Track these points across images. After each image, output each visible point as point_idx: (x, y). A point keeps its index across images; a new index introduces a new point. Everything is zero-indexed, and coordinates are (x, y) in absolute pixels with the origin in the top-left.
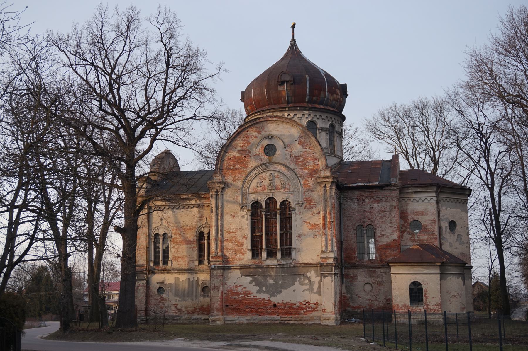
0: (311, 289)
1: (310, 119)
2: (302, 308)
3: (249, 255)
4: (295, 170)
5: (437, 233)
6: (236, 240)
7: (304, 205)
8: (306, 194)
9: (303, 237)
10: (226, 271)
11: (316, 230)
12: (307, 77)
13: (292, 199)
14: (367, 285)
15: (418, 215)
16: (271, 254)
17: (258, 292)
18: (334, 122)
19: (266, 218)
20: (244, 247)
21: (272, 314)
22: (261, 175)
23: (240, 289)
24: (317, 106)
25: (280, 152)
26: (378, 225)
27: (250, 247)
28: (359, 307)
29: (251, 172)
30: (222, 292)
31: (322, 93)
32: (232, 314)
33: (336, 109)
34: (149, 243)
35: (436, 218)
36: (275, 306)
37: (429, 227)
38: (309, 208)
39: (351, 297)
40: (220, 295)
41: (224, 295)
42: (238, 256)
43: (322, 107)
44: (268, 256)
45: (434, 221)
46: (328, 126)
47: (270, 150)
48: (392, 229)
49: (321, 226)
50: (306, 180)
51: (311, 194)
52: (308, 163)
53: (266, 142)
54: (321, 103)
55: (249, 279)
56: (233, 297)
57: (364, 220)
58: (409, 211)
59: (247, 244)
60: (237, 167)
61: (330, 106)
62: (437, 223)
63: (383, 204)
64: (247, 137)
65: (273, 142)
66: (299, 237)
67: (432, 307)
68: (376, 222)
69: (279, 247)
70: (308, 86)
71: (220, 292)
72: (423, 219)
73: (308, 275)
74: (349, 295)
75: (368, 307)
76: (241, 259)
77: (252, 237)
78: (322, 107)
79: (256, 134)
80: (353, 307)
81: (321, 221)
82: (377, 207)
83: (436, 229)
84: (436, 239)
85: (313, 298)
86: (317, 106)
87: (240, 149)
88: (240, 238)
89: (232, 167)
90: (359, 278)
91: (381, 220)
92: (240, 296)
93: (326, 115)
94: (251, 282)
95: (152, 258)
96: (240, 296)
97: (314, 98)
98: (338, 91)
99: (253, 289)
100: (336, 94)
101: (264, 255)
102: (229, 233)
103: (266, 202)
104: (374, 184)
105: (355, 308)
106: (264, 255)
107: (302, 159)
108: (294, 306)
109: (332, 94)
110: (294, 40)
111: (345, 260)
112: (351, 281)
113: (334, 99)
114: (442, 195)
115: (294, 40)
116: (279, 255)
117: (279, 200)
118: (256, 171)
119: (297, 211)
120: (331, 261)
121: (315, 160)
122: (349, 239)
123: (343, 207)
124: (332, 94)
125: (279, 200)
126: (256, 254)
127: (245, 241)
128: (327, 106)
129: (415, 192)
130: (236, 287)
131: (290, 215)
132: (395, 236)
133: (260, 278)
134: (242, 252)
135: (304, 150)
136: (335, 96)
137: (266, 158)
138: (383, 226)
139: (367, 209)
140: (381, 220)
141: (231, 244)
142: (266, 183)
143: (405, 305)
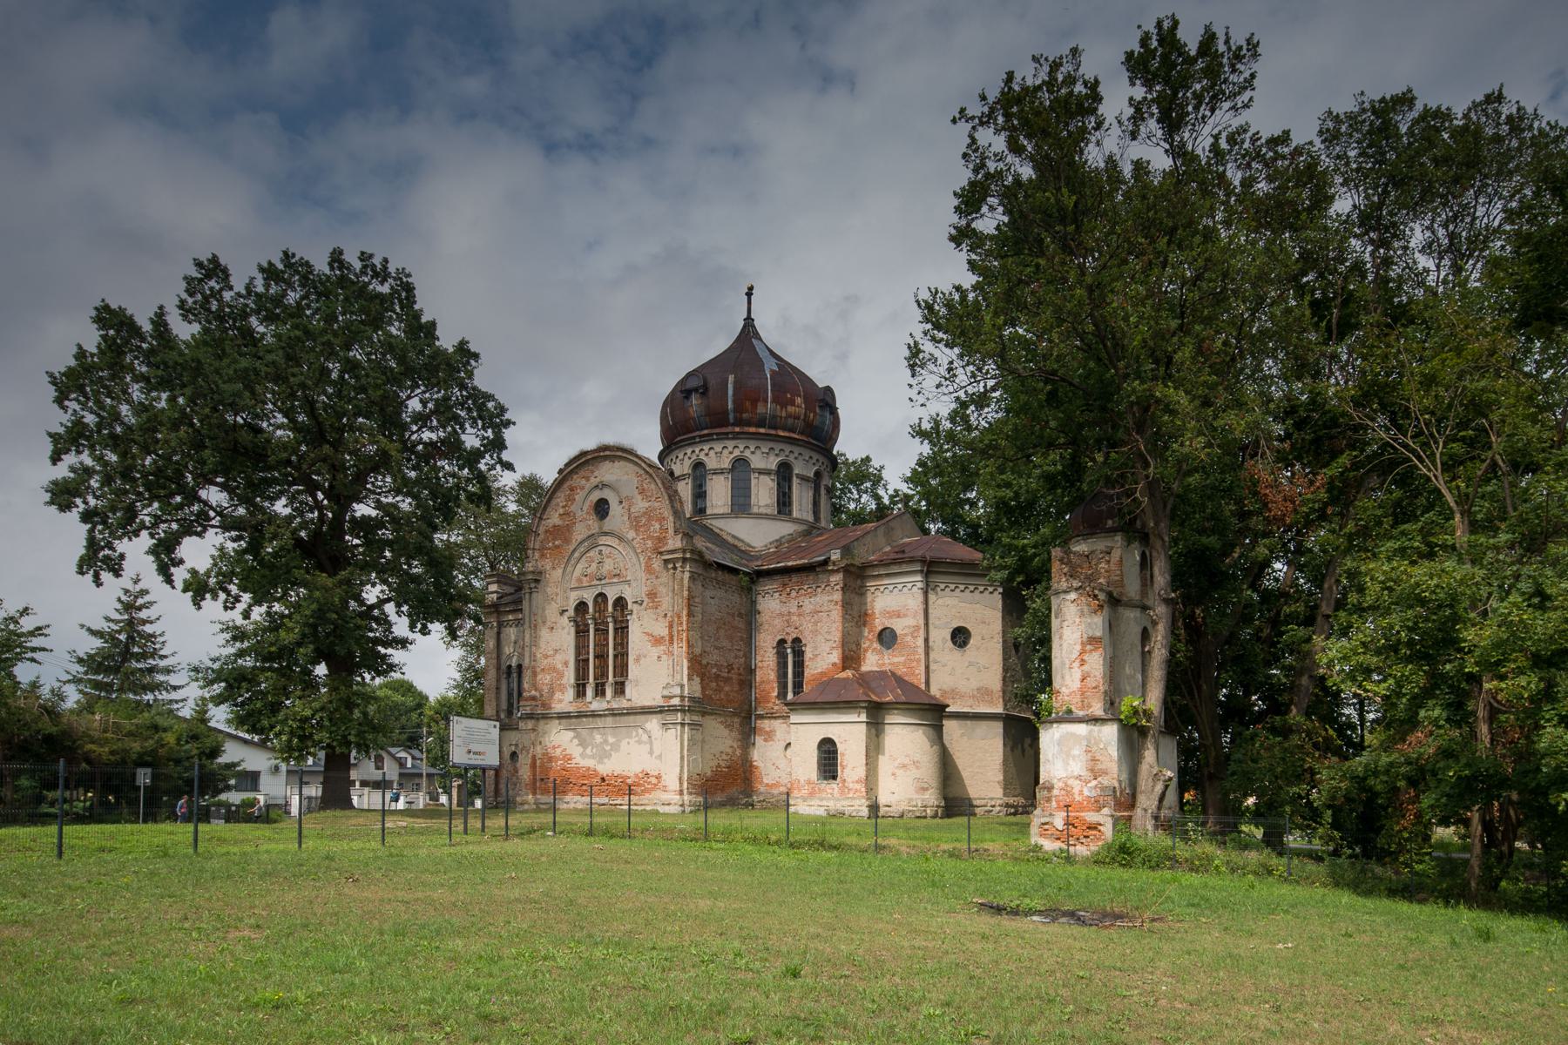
0: (651, 752)
1: (737, 453)
2: (638, 785)
3: (570, 694)
5: (921, 650)
10: (542, 722)
12: (731, 378)
16: (600, 691)
17: (583, 755)
18: (791, 458)
19: (596, 630)
20: (564, 681)
24: (752, 430)
25: (615, 509)
30: (534, 757)
33: (802, 433)
34: (498, 681)
35: (922, 622)
36: (603, 779)
43: (762, 430)
45: (917, 628)
46: (774, 467)
47: (601, 508)
54: (761, 424)
55: (571, 734)
59: (570, 677)
61: (784, 429)
62: (922, 633)
66: (637, 660)
68: (806, 633)
70: (730, 392)
72: (899, 626)
73: (648, 726)
77: (577, 661)
78: (762, 430)
79: (583, 482)
81: (665, 632)
82: (809, 604)
83: (920, 642)
84: (918, 661)
85: (652, 766)
86: (752, 430)
88: (559, 666)
93: (771, 445)
95: (504, 706)
98: (799, 400)
100: (793, 404)
102: (546, 657)
109: (784, 405)
110: (749, 320)
113: (789, 416)
115: (749, 320)
116: (609, 692)
120: (676, 701)
121: (662, 519)
126: (580, 691)
128: (775, 428)
129: (888, 575)
133: (584, 733)
134: (562, 689)
136: (791, 409)
139: (794, 610)
143: (809, 782)
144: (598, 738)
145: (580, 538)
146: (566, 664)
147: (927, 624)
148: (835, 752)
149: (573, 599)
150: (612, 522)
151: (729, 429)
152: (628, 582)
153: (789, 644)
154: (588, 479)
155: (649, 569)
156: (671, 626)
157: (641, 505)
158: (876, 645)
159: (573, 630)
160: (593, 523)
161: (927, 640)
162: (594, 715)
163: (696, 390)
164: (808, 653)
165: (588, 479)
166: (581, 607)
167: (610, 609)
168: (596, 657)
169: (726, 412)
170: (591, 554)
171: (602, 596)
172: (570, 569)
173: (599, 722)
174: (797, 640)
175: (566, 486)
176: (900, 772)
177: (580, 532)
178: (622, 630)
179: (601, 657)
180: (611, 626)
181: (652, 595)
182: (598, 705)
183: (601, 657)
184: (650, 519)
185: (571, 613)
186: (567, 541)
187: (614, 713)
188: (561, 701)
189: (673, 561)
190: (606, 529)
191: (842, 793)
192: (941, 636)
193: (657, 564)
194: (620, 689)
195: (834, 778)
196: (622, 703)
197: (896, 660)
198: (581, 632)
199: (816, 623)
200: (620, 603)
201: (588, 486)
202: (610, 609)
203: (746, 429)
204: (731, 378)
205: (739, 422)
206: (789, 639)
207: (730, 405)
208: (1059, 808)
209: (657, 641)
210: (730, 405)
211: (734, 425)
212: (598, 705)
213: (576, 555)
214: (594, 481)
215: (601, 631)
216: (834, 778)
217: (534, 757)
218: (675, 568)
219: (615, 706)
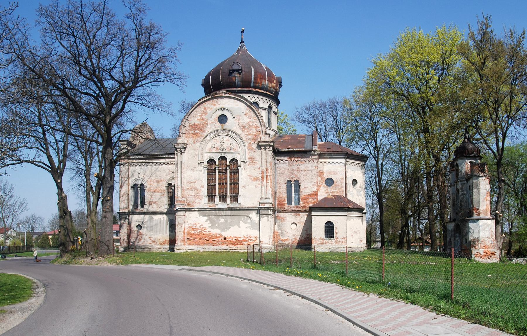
2: (245, 241)
4: (242, 136)
6: (195, 189)
7: (248, 163)
8: (250, 154)
9: (247, 187)
11: (258, 182)
13: (238, 157)
14: (294, 225)
15: (331, 174)
19: (219, 172)
20: (202, 194)
21: (223, 244)
22: (215, 138)
23: (198, 226)
24: (259, 91)
26: (302, 180)
27: (206, 194)
28: (287, 240)
29: (207, 136)
30: (184, 229)
31: (263, 81)
32: (192, 244)
36: (225, 238)
37: (339, 183)
38: (252, 165)
39: (282, 233)
40: (183, 230)
41: (186, 230)
42: (197, 200)
43: (263, 91)
44: (220, 200)
47: (222, 119)
48: (313, 183)
49: (261, 178)
50: (250, 143)
51: (254, 154)
52: (252, 131)
53: (220, 113)
54: (262, 89)
55: (206, 218)
56: (193, 232)
57: (292, 176)
58: (325, 171)
60: (196, 131)
63: (307, 165)
64: (205, 108)
65: (225, 113)
67: (340, 240)
68: (301, 178)
69: (229, 194)
71: (183, 228)
73: (251, 216)
74: (280, 231)
75: (293, 240)
76: (199, 203)
78: (263, 91)
79: (212, 106)
80: (282, 240)
81: (260, 175)
84: (343, 192)
86: (259, 91)
87: (199, 117)
88: (198, 187)
89: (193, 132)
90: (287, 219)
91: (305, 177)
92: (199, 231)
94: (206, 221)
96: (199, 231)
97: (257, 84)
98: (275, 81)
99: (207, 225)
101: (217, 199)
103: (219, 159)
104: (300, 149)
105: (284, 241)
106: (217, 199)
107: (247, 127)
108: (239, 239)
109: (271, 82)
111: (278, 206)
112: (282, 221)
114: (348, 160)
116: (228, 200)
117: (229, 158)
118: (211, 136)
119: (242, 167)
120: (267, 205)
122: (281, 190)
123: (277, 166)
124: (271, 82)
125: (229, 158)
127: (203, 189)
130: (196, 224)
131: (238, 169)
132: (315, 189)
133: (214, 218)
134: (200, 198)
135: (249, 120)
136: (273, 84)
137: (220, 125)
138: (306, 181)
139: (295, 168)
140: (305, 177)
141: (191, 192)
142: (218, 145)
143: (321, 239)
144: (222, 220)
145: (210, 131)
146: (202, 187)
147: (346, 178)
148: (333, 226)
149: (206, 158)
150: (227, 126)
151: (250, 89)
152: (239, 153)
153: (293, 182)
154: (215, 105)
155: (250, 148)
156: (262, 174)
157: (245, 120)
158: (324, 184)
159: (206, 171)
160: (218, 126)
161: (346, 184)
162: (220, 210)
163: (238, 71)
164: (302, 186)
165: (215, 105)
166: (211, 161)
167: (228, 163)
168: (219, 184)
169: (250, 82)
170: (217, 138)
171: (223, 158)
172: (204, 143)
173: (222, 213)
174: (297, 181)
175: (201, 106)
176: (354, 235)
177: (209, 129)
178: (235, 172)
179: (223, 184)
180: (228, 171)
181: (252, 159)
182: (221, 205)
183: (223, 184)
184: (250, 127)
185: (205, 164)
186: (202, 131)
187: (231, 209)
188: (199, 203)
189: (265, 146)
190: (225, 128)
191: (336, 243)
192: (350, 182)
193: (254, 146)
194: (235, 198)
195: (333, 237)
196: (234, 205)
197: (333, 191)
198: (211, 173)
199: (306, 175)
200: (234, 161)
201: (215, 108)
202: (228, 163)
203: (257, 90)
204: (252, 68)
205: (255, 87)
206: (293, 180)
207: (253, 79)
208: (481, 247)
209: (255, 179)
210: (253, 79)
211: (252, 87)
212: (221, 205)
213: (208, 138)
214: (218, 107)
215: (223, 173)
216: (333, 237)
217: (184, 229)
218: (265, 149)
219: (231, 206)
